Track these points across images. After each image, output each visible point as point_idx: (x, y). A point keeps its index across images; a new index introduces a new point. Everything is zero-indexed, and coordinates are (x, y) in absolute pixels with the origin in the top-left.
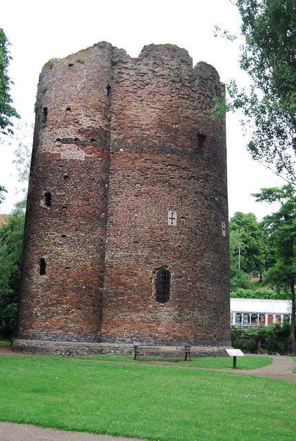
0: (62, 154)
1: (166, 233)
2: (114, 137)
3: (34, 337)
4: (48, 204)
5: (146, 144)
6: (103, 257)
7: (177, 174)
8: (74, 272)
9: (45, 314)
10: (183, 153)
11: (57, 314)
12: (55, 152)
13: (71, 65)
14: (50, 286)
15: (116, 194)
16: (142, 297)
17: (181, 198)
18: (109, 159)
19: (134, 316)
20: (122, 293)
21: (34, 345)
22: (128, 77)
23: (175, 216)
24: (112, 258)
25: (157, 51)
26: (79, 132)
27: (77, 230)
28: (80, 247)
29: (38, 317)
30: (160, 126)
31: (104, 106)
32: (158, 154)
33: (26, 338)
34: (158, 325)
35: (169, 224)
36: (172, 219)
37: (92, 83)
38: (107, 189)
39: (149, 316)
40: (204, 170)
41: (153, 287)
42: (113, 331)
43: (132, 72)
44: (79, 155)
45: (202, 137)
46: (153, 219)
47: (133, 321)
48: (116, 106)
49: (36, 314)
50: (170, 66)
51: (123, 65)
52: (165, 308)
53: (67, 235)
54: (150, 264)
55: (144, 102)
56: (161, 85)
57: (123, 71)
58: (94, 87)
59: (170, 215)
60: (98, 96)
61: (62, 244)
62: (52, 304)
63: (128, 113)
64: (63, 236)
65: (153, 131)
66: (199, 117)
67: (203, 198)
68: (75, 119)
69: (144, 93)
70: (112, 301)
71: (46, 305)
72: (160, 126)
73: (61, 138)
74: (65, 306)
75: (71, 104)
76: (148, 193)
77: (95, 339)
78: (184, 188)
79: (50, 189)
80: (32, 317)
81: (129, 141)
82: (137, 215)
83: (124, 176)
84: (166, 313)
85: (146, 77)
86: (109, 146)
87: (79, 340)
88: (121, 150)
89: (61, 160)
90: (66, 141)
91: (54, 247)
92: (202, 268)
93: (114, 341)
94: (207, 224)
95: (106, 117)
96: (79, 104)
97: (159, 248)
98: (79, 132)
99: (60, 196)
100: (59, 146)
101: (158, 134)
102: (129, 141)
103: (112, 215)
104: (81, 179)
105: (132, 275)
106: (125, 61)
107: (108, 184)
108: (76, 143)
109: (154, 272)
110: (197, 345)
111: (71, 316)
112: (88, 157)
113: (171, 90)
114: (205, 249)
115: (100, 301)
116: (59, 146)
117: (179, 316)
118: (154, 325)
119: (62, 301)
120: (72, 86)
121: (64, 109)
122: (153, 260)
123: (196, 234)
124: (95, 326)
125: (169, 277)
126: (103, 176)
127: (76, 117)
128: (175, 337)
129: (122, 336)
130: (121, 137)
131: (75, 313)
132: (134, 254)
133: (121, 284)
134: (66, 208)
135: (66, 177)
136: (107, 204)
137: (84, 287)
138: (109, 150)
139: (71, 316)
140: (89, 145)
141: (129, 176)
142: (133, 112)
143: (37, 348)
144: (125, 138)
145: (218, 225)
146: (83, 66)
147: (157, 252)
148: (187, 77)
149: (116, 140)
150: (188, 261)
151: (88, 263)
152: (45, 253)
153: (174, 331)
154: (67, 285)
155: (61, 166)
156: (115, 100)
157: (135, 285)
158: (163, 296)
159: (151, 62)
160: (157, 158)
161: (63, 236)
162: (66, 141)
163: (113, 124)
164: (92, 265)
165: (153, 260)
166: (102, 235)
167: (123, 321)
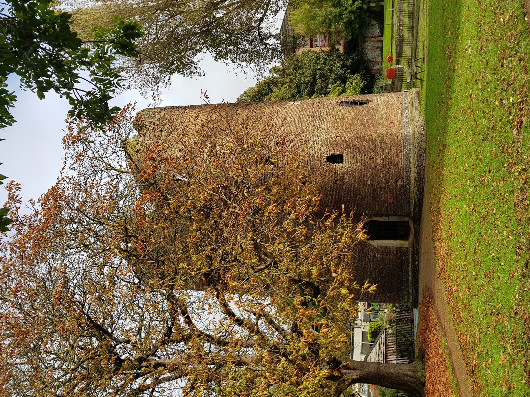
9: (383, 149)
29: (386, 157)
33: (409, 171)
49: (383, 160)
53: (305, 139)
62: (373, 144)
71: (374, 150)
80: (387, 166)
91: (316, 148)
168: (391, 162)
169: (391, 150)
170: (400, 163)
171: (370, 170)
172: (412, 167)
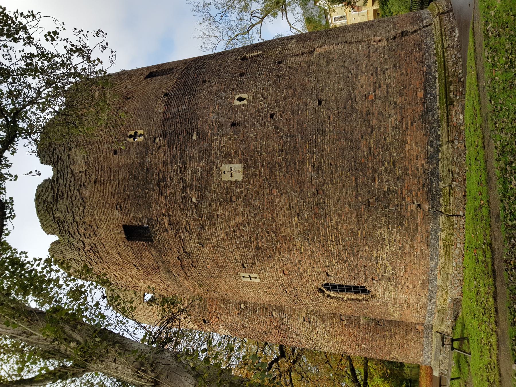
92: (306, 239)
114: (275, 233)
117: (389, 280)
164: (335, 336)
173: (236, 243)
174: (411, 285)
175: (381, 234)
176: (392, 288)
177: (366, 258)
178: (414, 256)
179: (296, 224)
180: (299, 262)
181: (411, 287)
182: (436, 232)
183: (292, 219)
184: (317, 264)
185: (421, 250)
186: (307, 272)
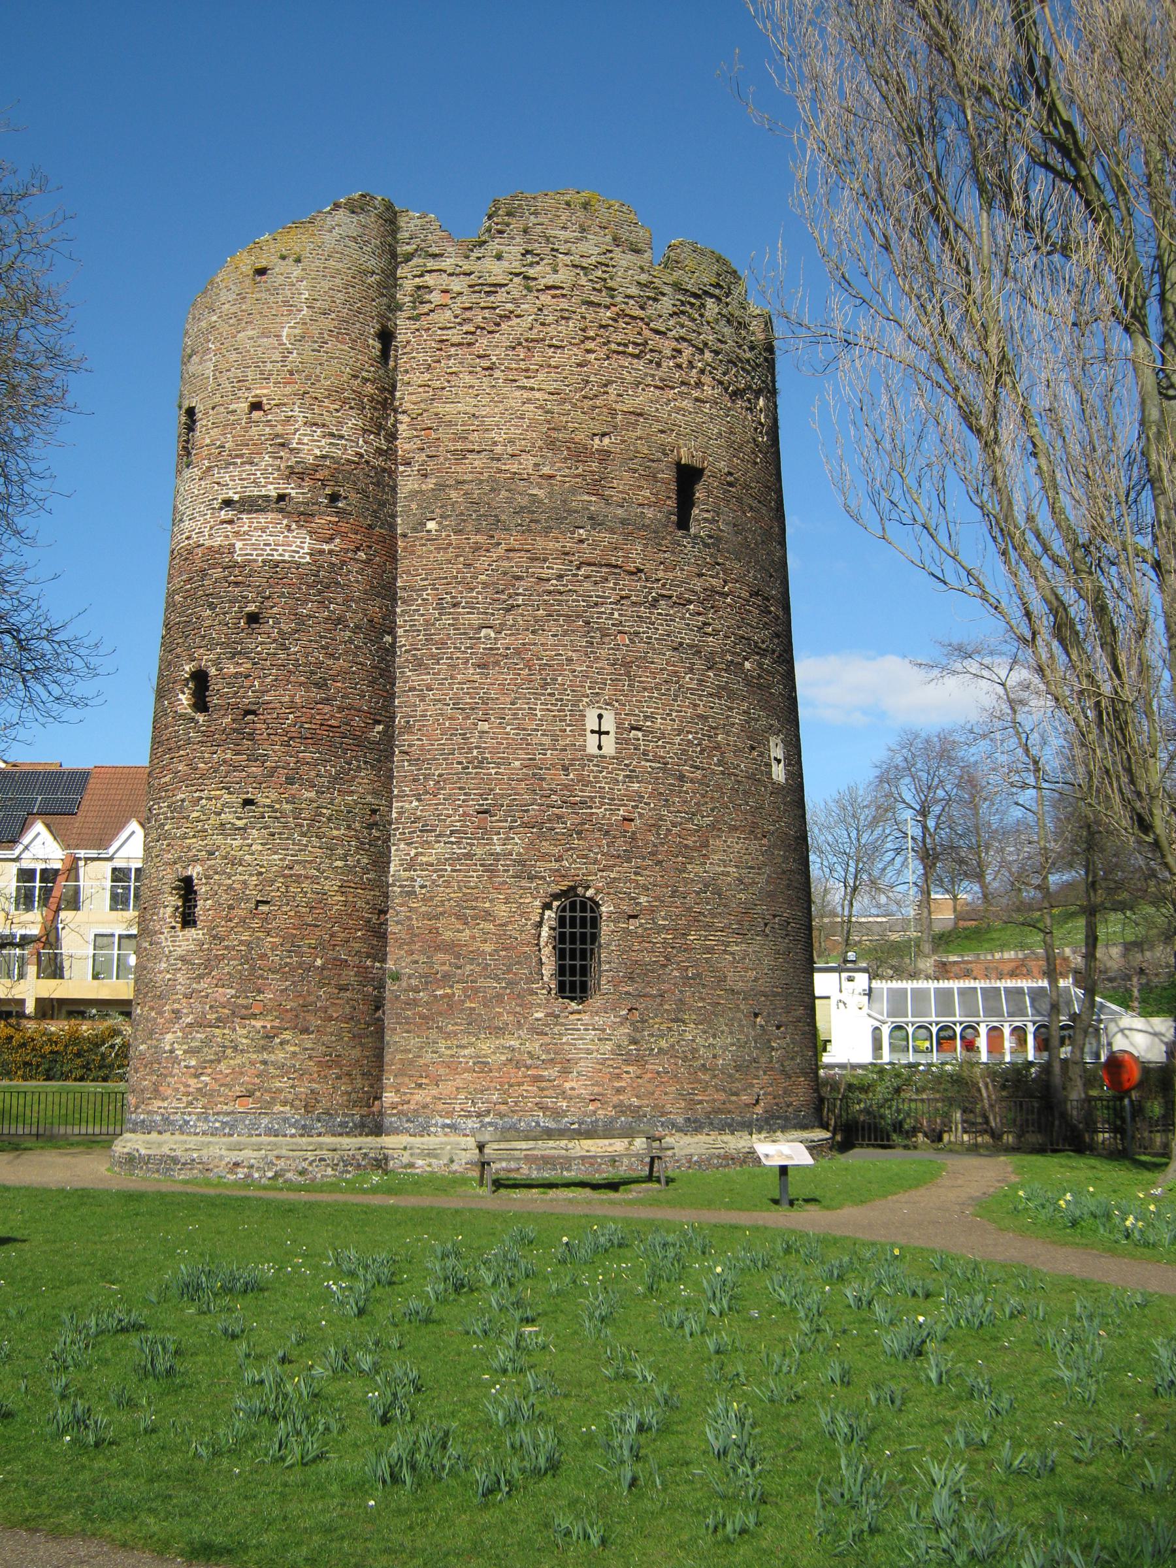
0: (239, 545)
1: (582, 780)
2: (407, 483)
3: (167, 1124)
4: (200, 704)
5: (509, 501)
6: (381, 862)
7: (609, 590)
8: (283, 919)
10: (630, 528)
11: (235, 1048)
12: (218, 541)
13: (261, 272)
14: (209, 964)
15: (419, 665)
16: (510, 983)
17: (626, 664)
18: (393, 558)
19: (486, 1046)
20: (447, 976)
21: (165, 1150)
22: (446, 299)
23: (609, 724)
24: (411, 867)
25: (536, 214)
26: (295, 474)
27: (290, 781)
28: (304, 835)
29: (176, 1061)
30: (551, 444)
31: (369, 389)
32: (547, 530)
34: (565, 1072)
35: (592, 749)
36: (600, 731)
37: (327, 323)
38: (391, 650)
39: (534, 1046)
40: (700, 575)
41: (547, 952)
42: (420, 1097)
43: (457, 285)
44: (293, 545)
45: (688, 477)
46: (538, 738)
47: (482, 1066)
48: (406, 397)
49: (172, 1051)
50: (577, 260)
51: (431, 264)
52: (585, 1017)
53: (261, 800)
54: (531, 878)
55: (497, 374)
56: (550, 319)
57: (429, 280)
58: (338, 335)
59: (591, 723)
60: (346, 361)
61: (244, 829)
62: (218, 1019)
63: (449, 408)
64: (248, 802)
65: (528, 461)
66: (679, 410)
67: (699, 664)
68: (277, 436)
69: (495, 346)
70: (415, 1003)
71: (200, 1024)
72: (551, 444)
73: (236, 497)
74: (258, 1024)
75: (260, 391)
76: (518, 652)
77: (362, 1125)
78: (637, 633)
79: (206, 659)
81: (454, 494)
82: (485, 726)
83: (440, 607)
84: (591, 1034)
85: (501, 295)
86: (394, 516)
87: (306, 1131)
88: (431, 525)
89: (236, 565)
90: (251, 505)
92: (706, 886)
93: (424, 1130)
94: (717, 747)
95: (380, 427)
96: (289, 389)
97: (559, 828)
98: (295, 474)
99: (237, 675)
100: (231, 522)
101: (546, 470)
102: (454, 494)
103: (408, 728)
104: (300, 620)
105: (474, 918)
106: (435, 250)
107: (392, 632)
108: (281, 510)
109: (547, 906)
110: (698, 1130)
111: (280, 1056)
112: (322, 552)
113: (583, 330)
114: (712, 826)
115: (378, 1004)
116: (231, 522)
117: (634, 1042)
118: (551, 1072)
119: (246, 1007)
120: (264, 335)
121: (245, 406)
122: (542, 867)
123: (682, 778)
124: (359, 1082)
125: (595, 922)
126: (374, 609)
127: (279, 429)
128: (621, 1108)
129: (449, 1114)
130: (431, 483)
131: (290, 1049)
132: (479, 851)
133: (438, 948)
134: (254, 713)
135: (253, 618)
136: (392, 696)
137: (319, 962)
138: (392, 527)
139: (280, 1056)
140: (323, 513)
141: (455, 605)
142: (465, 405)
143: (175, 1160)
144: (441, 487)
145: (757, 743)
146: (297, 272)
147: (556, 842)
148: (634, 291)
149: (413, 494)
150: (659, 863)
151: (331, 885)
152: (195, 860)
153: (619, 1091)
154: (263, 956)
155: (237, 584)
156: (407, 372)
157: (488, 948)
158: (574, 981)
159: (517, 250)
160: (540, 543)
161: (248, 802)
162: (251, 505)
163: (403, 446)
165: (542, 867)
166: (375, 793)
167: (453, 1066)
168: (166, 1076)
169: (197, 1076)
170: (160, 1104)
171: (153, 1014)
172: (147, 1137)
173: (688, 732)
174: (623, 1084)
175: (722, 1032)
176: (608, 1046)
177: (680, 1000)
178: (692, 1089)
179: (728, 874)
180: (659, 863)
181: (616, 1084)
182: (730, 1126)
183: (736, 867)
184: (657, 898)
185: (701, 1102)
186: (636, 874)
